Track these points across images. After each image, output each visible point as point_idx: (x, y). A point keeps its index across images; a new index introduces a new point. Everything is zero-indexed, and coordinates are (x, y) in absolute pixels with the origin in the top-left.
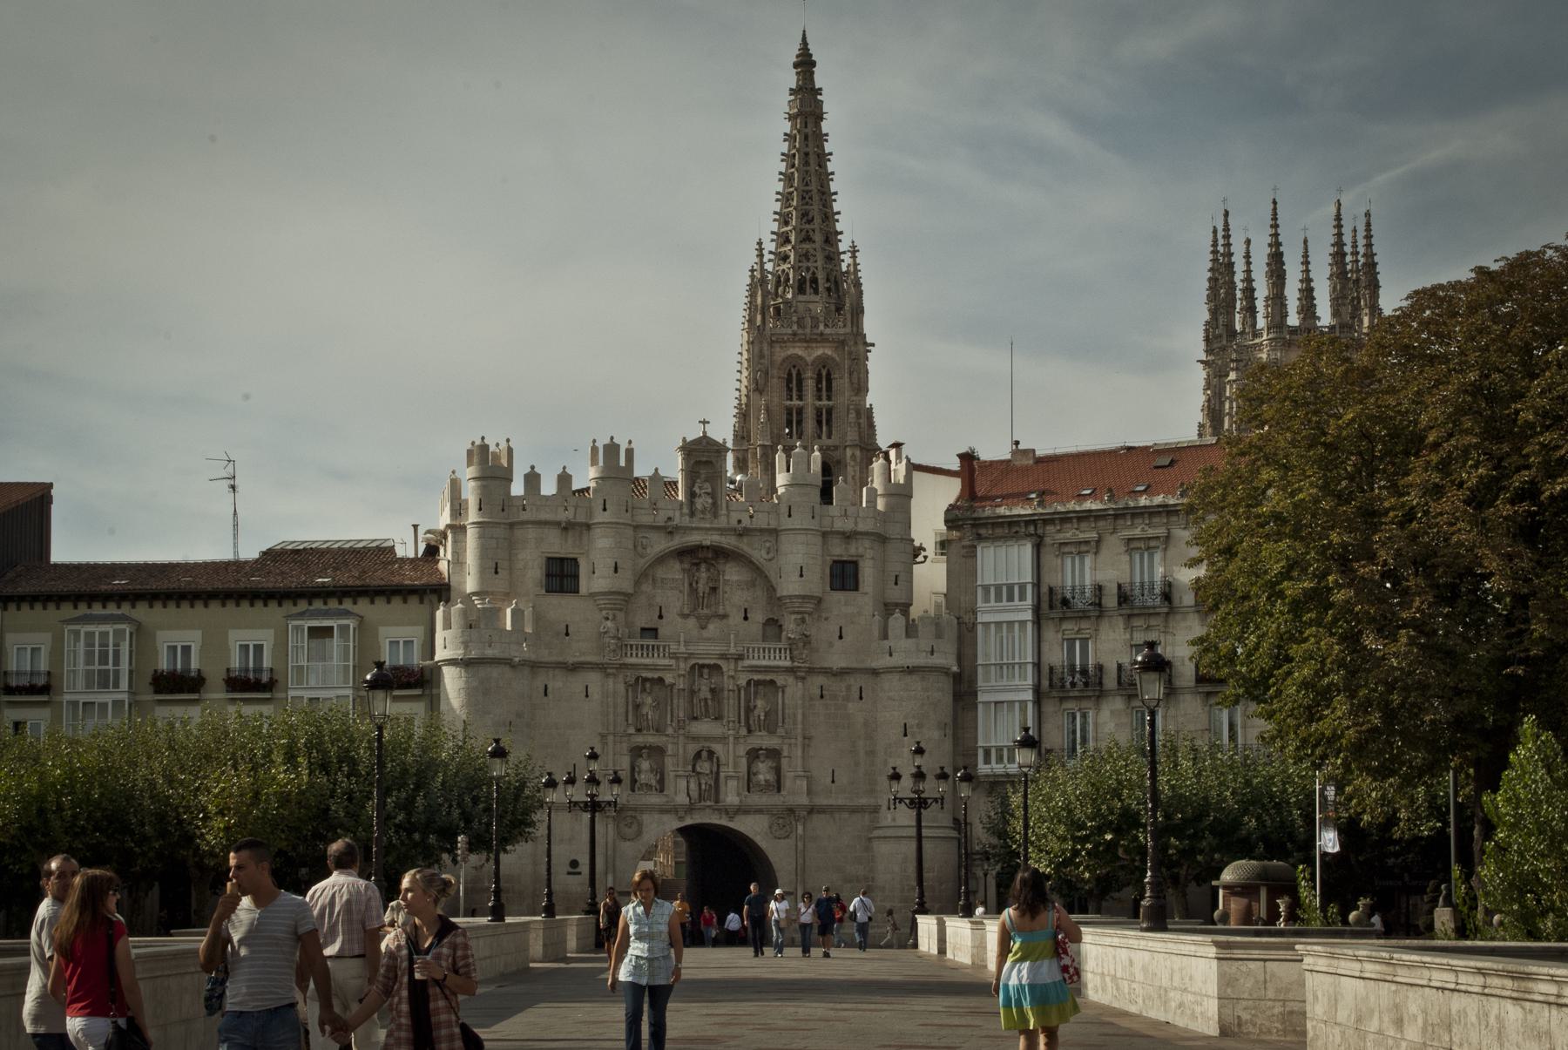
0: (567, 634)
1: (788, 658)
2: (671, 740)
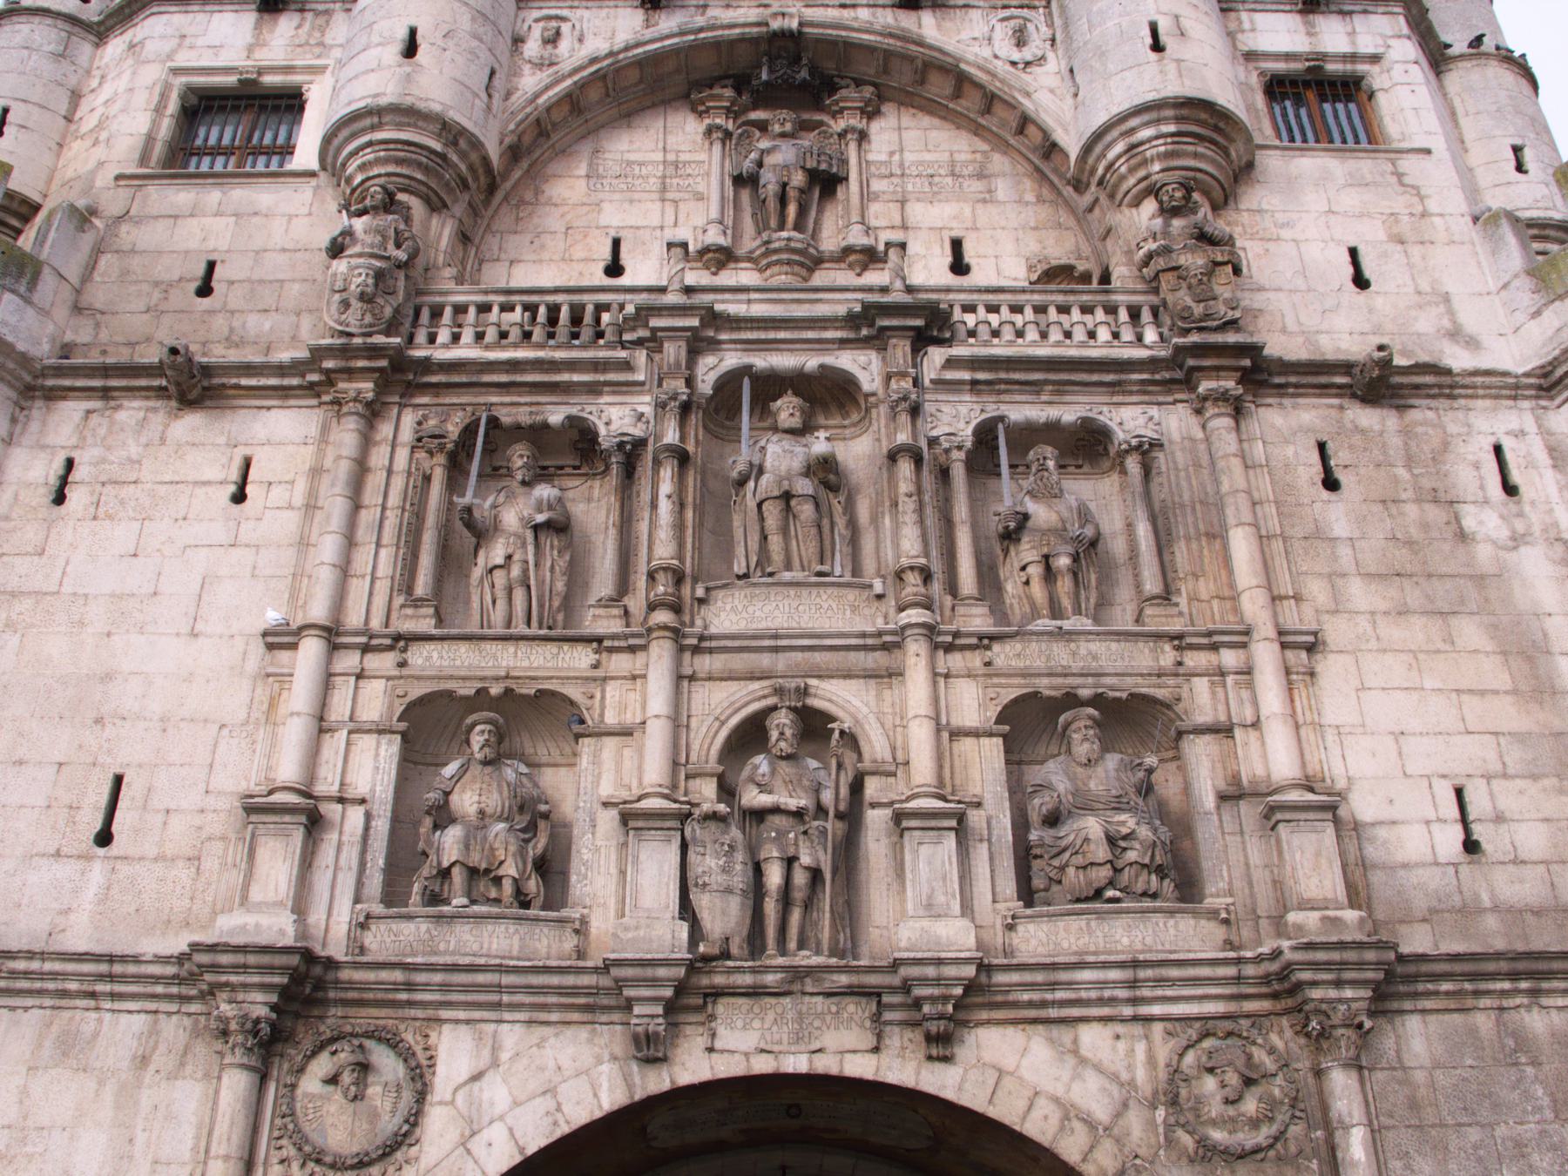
0: (205, 290)
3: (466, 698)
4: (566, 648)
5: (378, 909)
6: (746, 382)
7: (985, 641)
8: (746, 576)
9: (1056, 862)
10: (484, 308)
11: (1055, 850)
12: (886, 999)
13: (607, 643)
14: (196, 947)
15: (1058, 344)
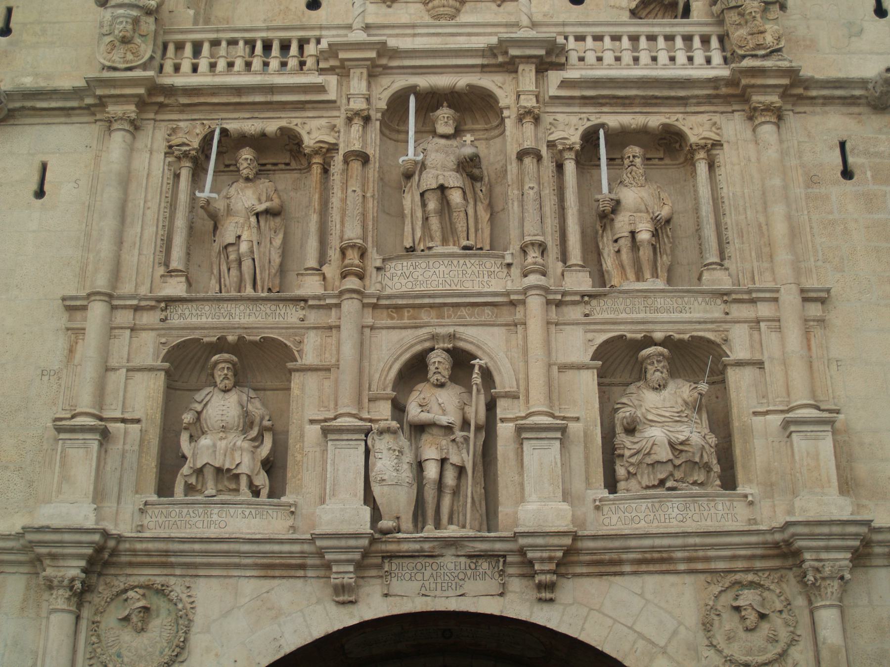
1: (717, 58)
2: (313, 318)
3: (210, 344)
4: (281, 306)
5: (154, 498)
6: (412, 100)
7: (587, 297)
8: (412, 249)
9: (633, 460)
10: (215, 43)
11: (632, 451)
12: (509, 559)
13: (310, 302)
14: (26, 529)
15: (646, 66)
